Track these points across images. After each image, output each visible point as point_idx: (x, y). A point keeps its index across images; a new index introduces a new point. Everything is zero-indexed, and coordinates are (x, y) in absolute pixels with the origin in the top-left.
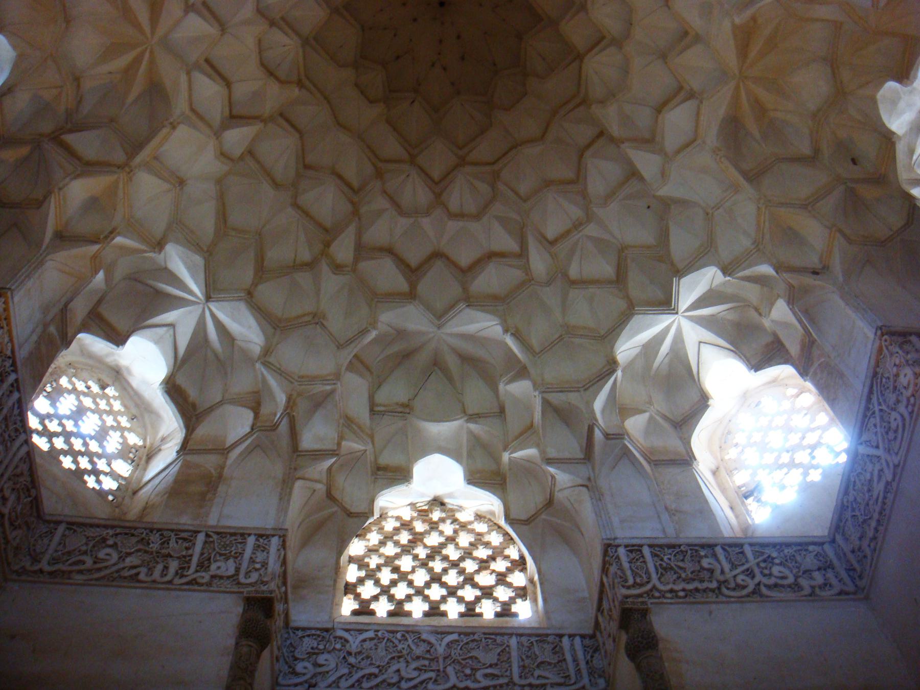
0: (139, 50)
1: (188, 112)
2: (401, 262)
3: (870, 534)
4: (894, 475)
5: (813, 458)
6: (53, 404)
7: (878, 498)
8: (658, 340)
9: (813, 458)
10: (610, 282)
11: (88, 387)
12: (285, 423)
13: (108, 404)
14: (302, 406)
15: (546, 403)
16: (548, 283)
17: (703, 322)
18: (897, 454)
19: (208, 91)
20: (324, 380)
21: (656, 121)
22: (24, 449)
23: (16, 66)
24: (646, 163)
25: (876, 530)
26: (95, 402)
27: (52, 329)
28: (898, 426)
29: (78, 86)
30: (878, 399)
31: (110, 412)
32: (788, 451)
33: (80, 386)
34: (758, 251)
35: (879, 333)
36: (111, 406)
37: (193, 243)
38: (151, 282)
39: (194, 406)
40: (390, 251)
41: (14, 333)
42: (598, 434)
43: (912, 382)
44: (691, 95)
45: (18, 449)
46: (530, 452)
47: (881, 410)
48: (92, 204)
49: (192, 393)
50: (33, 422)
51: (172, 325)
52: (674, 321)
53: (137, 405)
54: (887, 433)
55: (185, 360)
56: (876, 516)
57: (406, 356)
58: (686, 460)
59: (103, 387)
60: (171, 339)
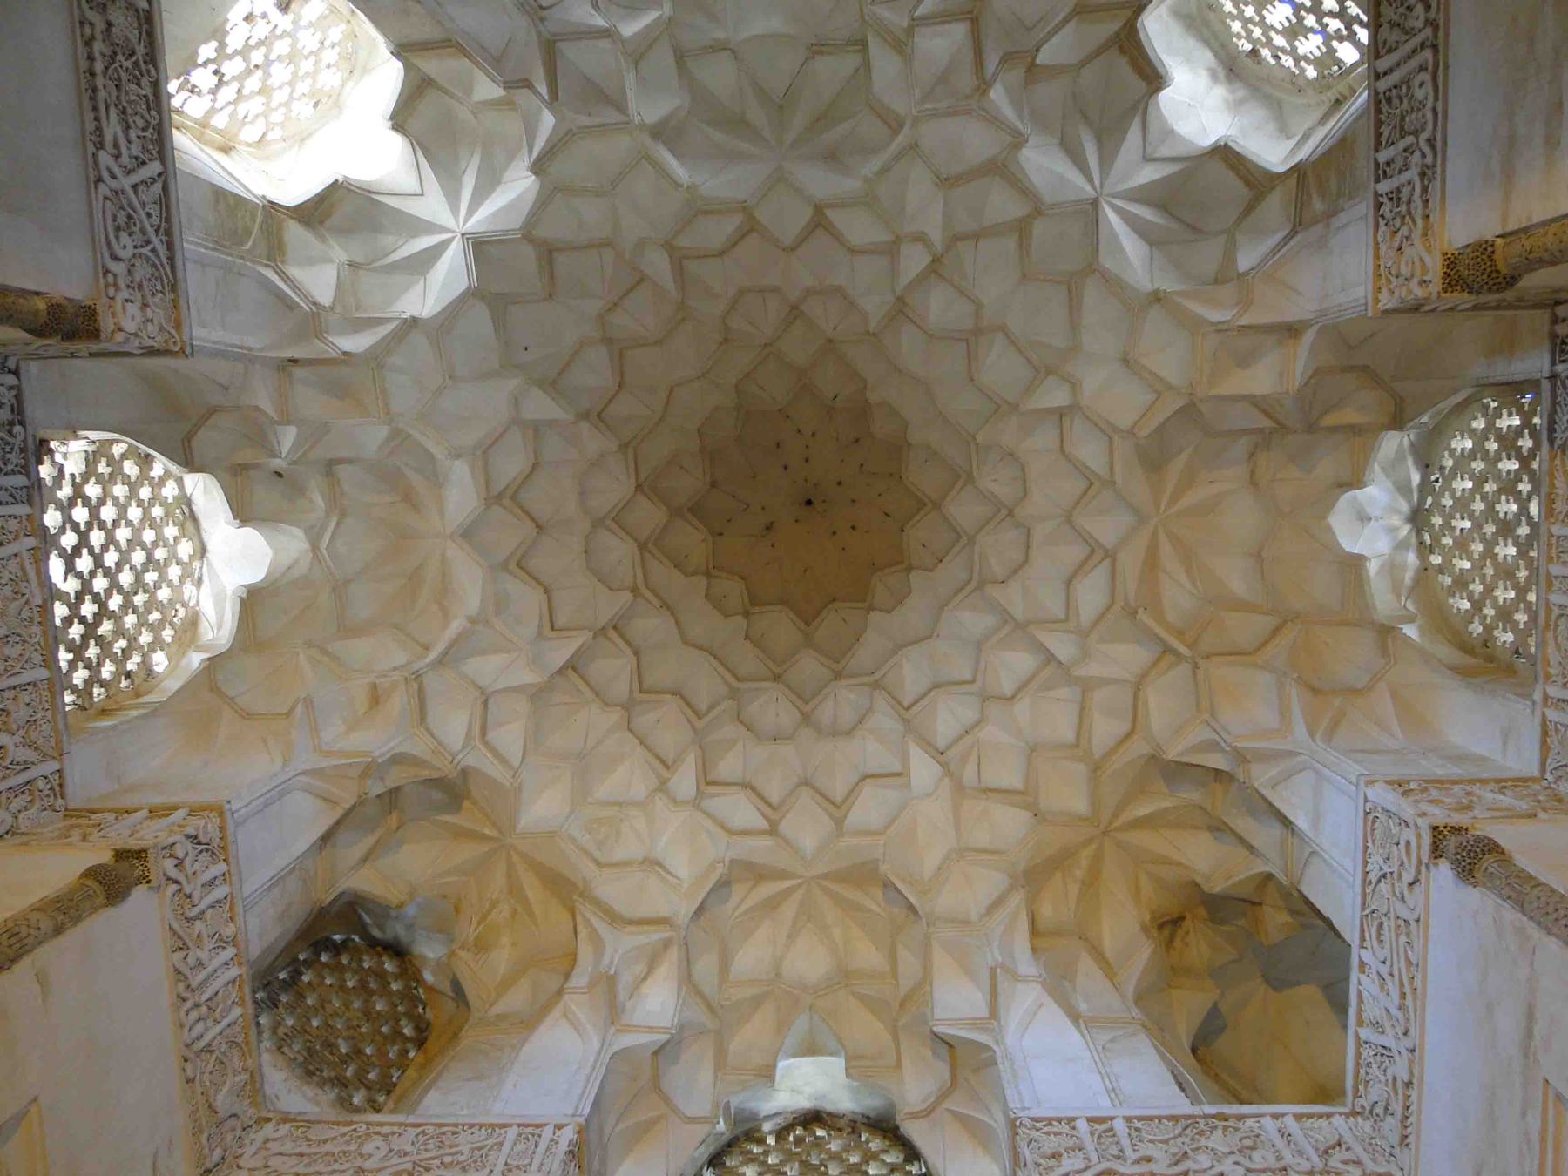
0: (1174, 509)
1: (1116, 438)
2: (837, 237)
3: (98, 46)
4: (96, 163)
5: (216, 72)
6: (1332, 52)
7: (107, 108)
8: (481, 193)
9: (216, 72)
10: (560, 250)
11: (1277, 57)
12: (990, 68)
13: (1249, 32)
14: (965, 80)
15: (621, 108)
16: (641, 244)
17: (422, 226)
18: (106, 198)
19: (1090, 452)
20: (935, 115)
21: (535, 453)
22: (1383, 64)
23: (1330, 506)
24: (541, 406)
25: (91, 58)
26: (1269, 40)
27: (1318, 205)
28: (117, 238)
29: (1252, 472)
30: (158, 256)
31: (1246, 22)
32: (257, 67)
33: (1288, 61)
34: (375, 358)
35: (188, 351)
36: (1244, 27)
37: (1114, 285)
38: (1174, 225)
39: (1122, 50)
40: (853, 251)
41: (1371, 252)
42: (543, 89)
43: (121, 315)
44: (499, 497)
45: (1391, 70)
46: (630, 28)
47: (148, 242)
48: (1244, 361)
49: (1123, 65)
50: (1363, 35)
51: (1148, 159)
52: (466, 221)
53: (1206, 23)
54: (129, 217)
55: (1134, 108)
56: (100, 81)
57: (823, 119)
58: (402, 50)
59: (1254, 53)
60: (1150, 137)
